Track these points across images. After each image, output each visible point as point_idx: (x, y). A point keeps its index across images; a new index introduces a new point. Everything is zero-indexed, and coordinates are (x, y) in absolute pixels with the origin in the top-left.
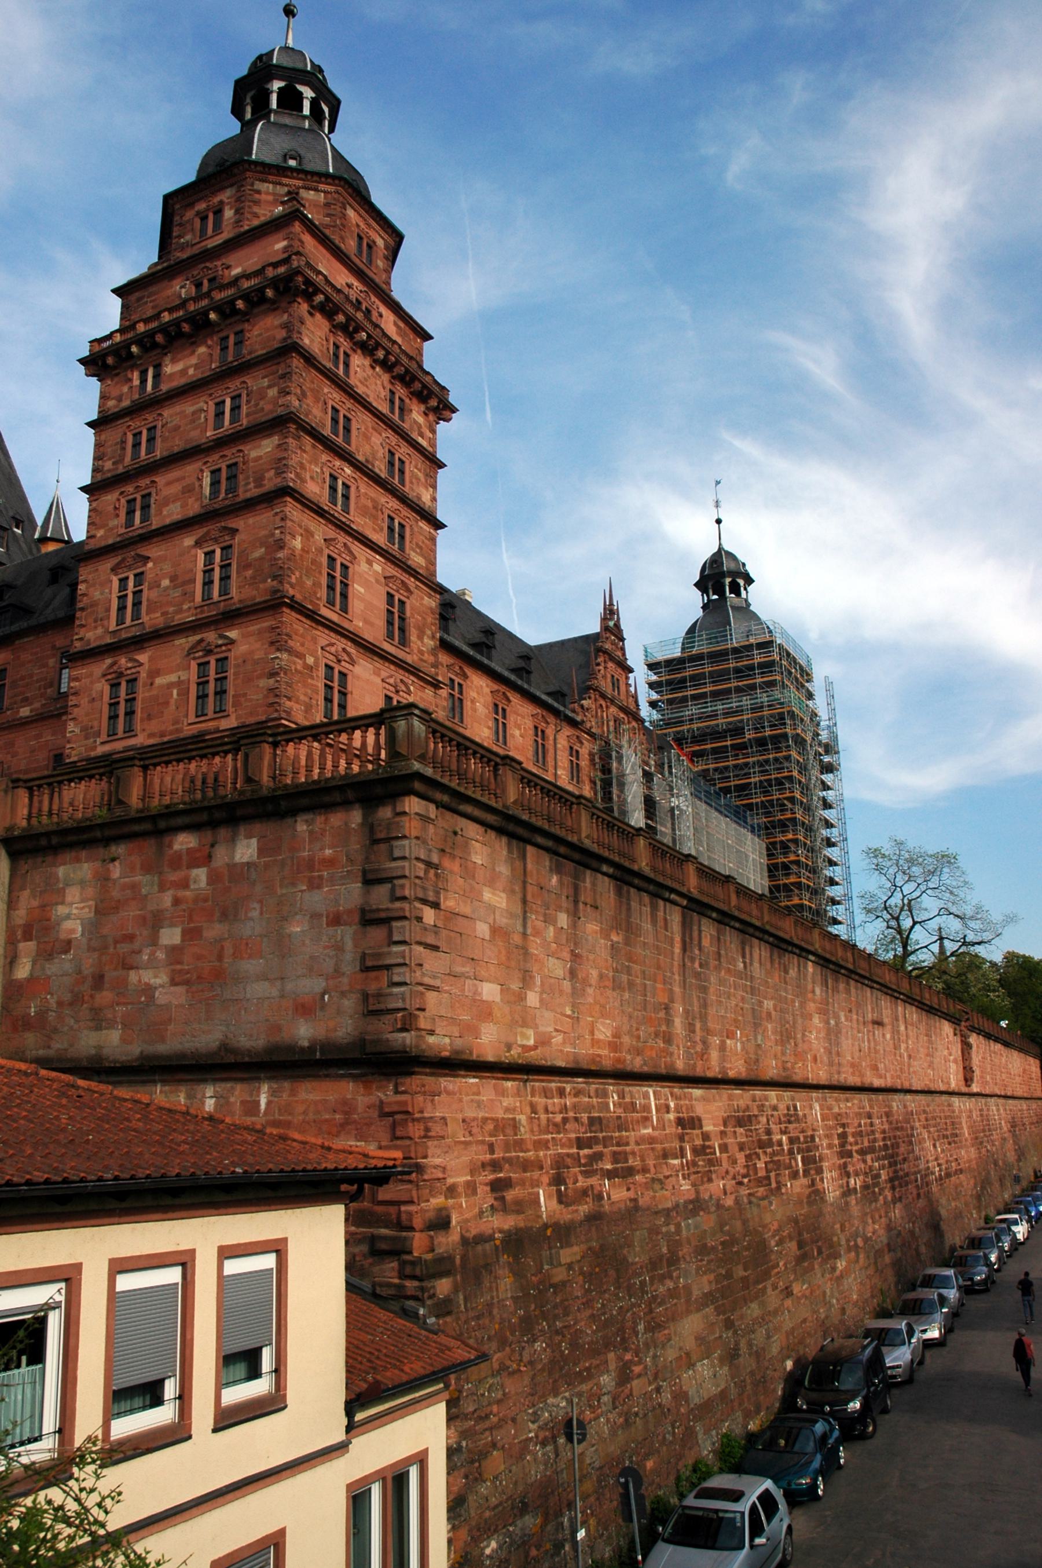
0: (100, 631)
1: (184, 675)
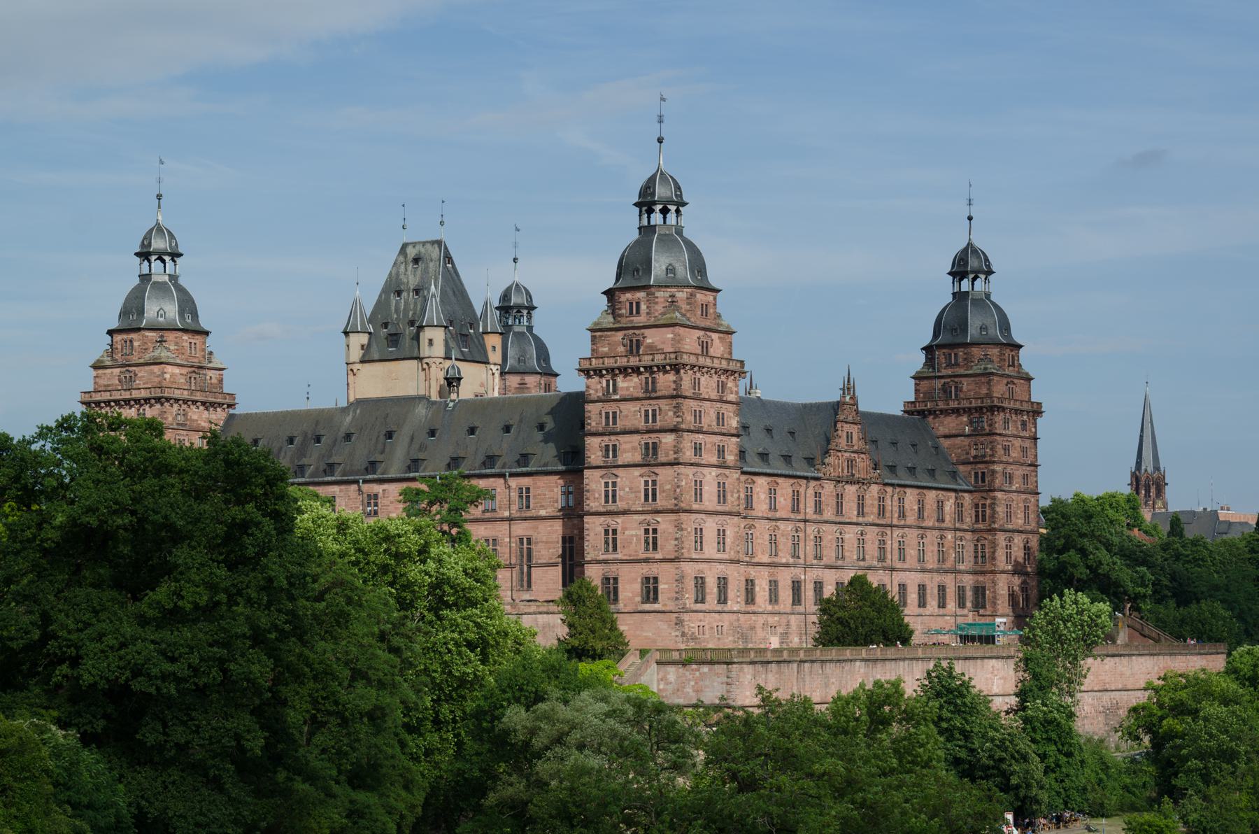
0: (597, 504)
1: (638, 533)
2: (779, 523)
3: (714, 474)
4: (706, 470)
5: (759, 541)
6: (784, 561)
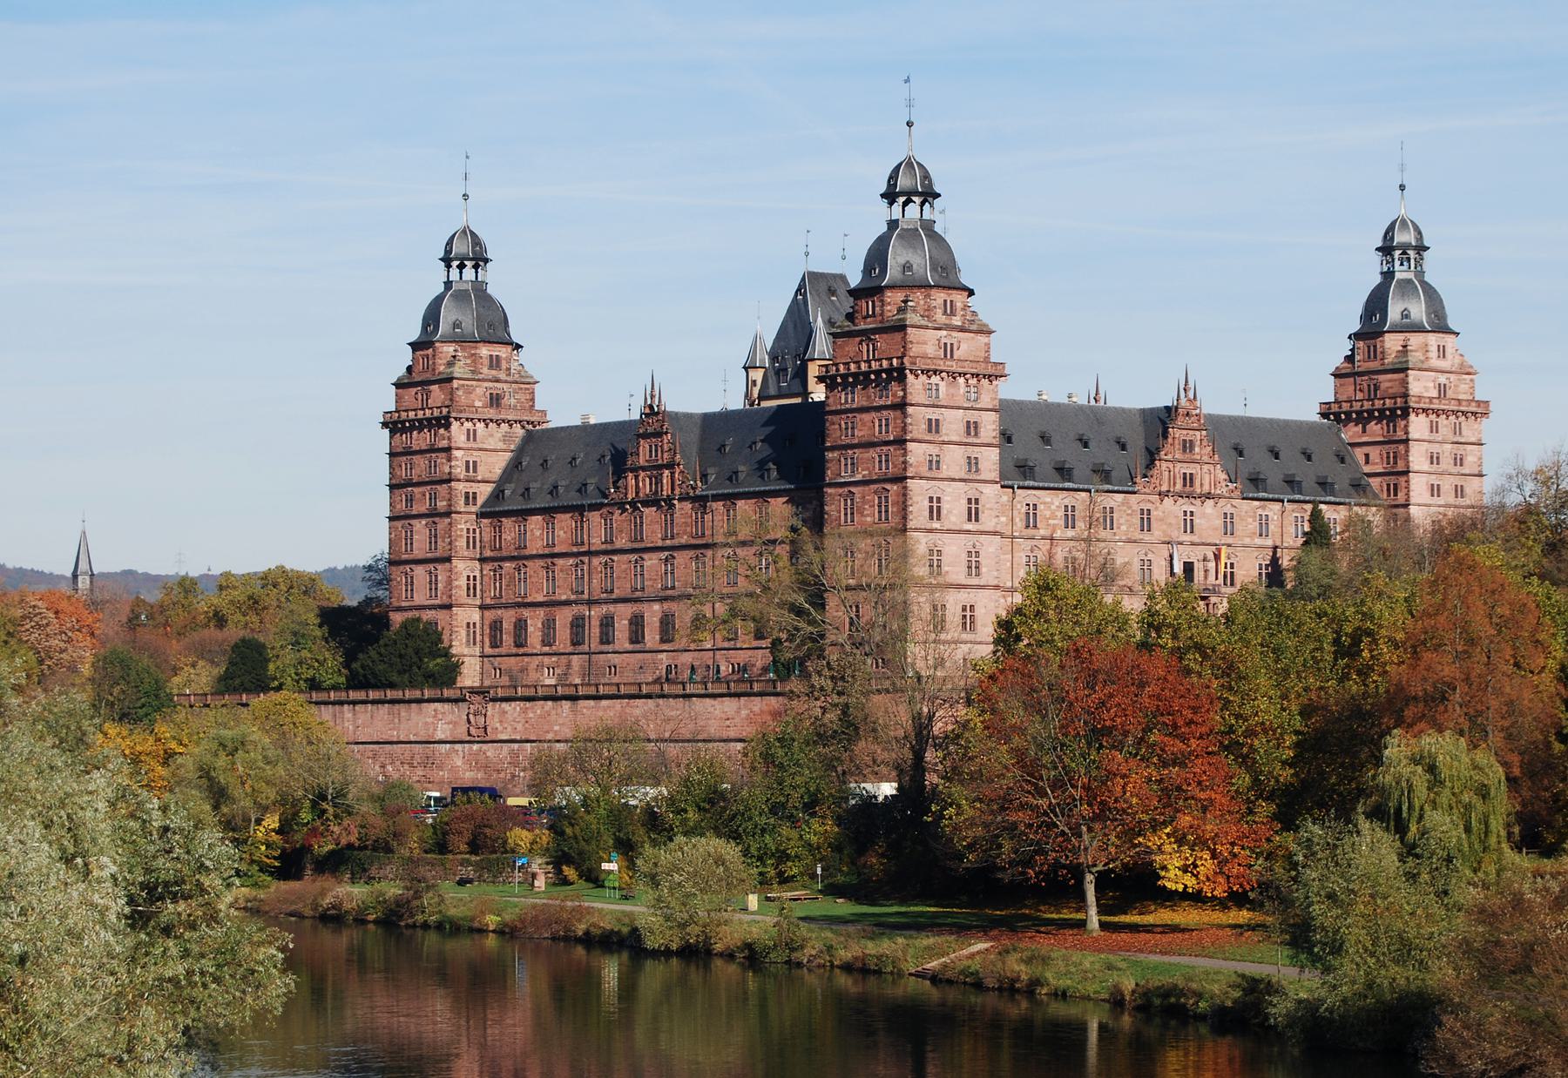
2: (556, 560)
3: (424, 522)
4: (413, 522)
5: (533, 580)
6: (564, 598)
